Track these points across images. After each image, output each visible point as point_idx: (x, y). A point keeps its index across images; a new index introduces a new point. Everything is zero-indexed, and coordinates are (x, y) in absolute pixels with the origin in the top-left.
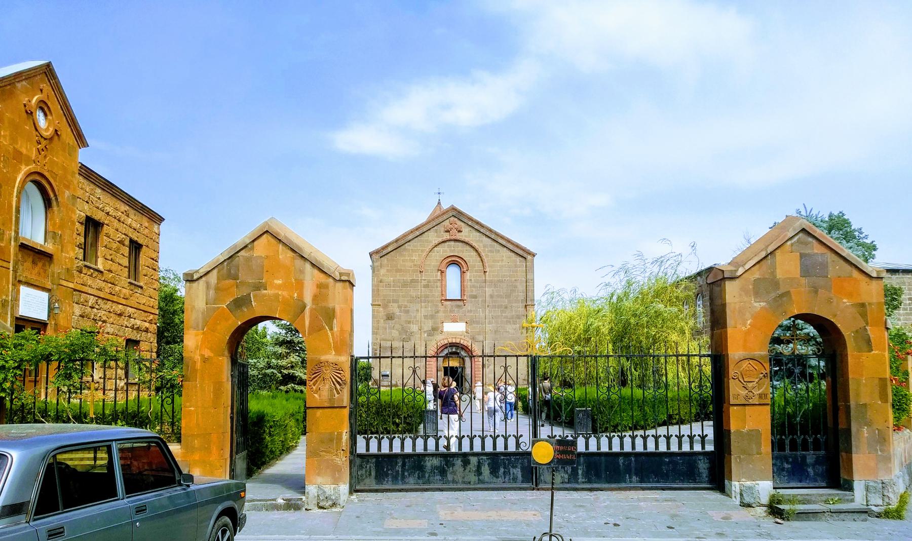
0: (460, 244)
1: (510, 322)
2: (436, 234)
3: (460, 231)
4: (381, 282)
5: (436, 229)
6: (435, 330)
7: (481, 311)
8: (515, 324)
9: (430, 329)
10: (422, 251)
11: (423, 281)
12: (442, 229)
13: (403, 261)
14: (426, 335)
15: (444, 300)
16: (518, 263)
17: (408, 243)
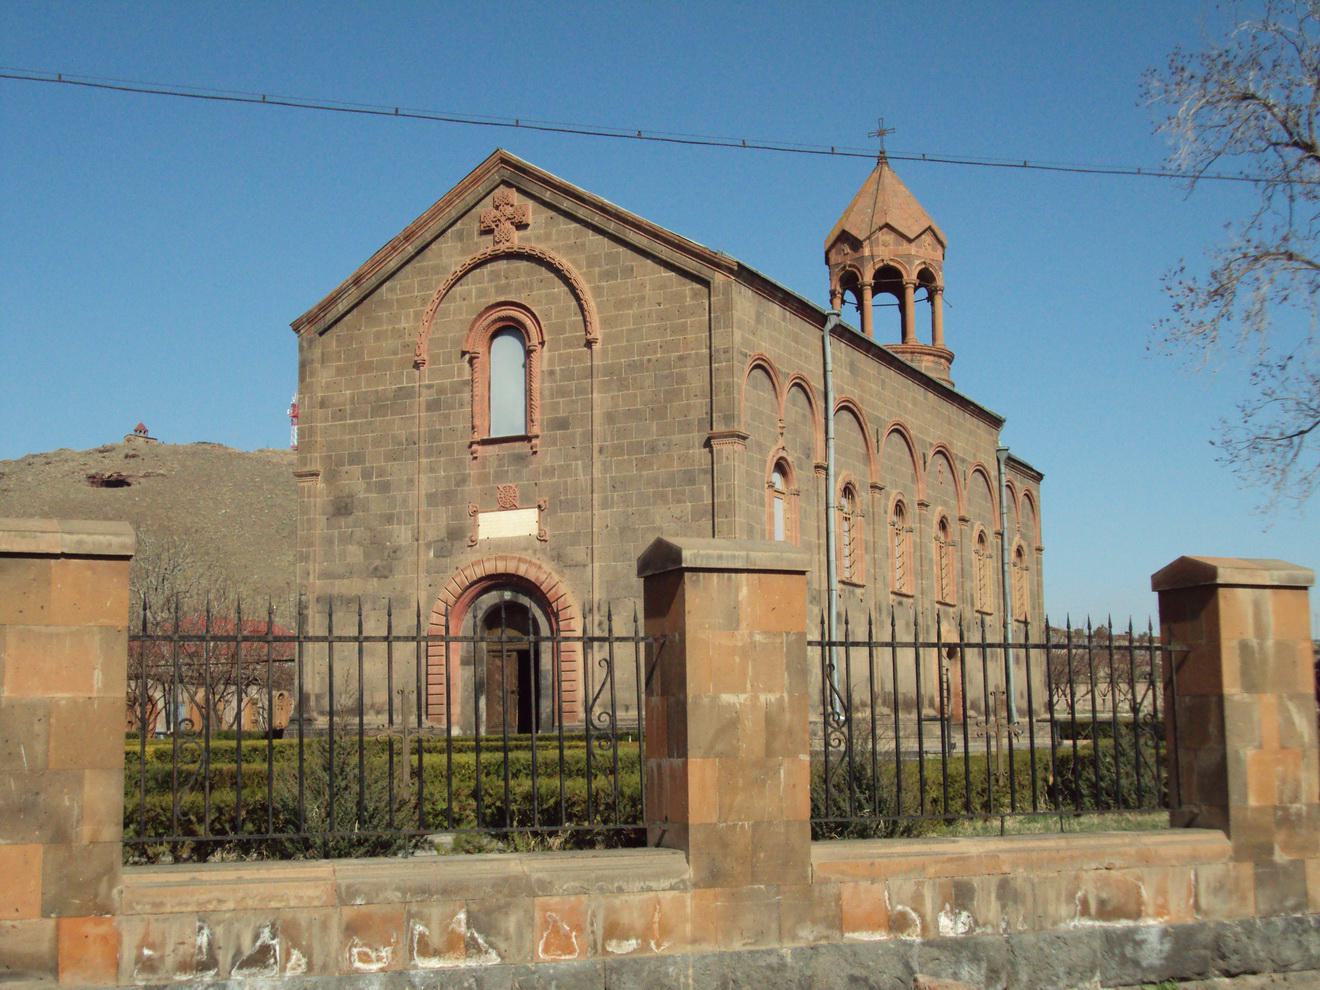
0: (523, 265)
1: (663, 497)
2: (459, 245)
3: (521, 226)
4: (323, 405)
5: (458, 231)
6: (458, 535)
7: (580, 467)
8: (679, 501)
9: (443, 534)
10: (424, 301)
11: (424, 391)
12: (476, 227)
13: (378, 337)
14: (432, 554)
15: (478, 443)
16: (688, 301)
17: (387, 284)
